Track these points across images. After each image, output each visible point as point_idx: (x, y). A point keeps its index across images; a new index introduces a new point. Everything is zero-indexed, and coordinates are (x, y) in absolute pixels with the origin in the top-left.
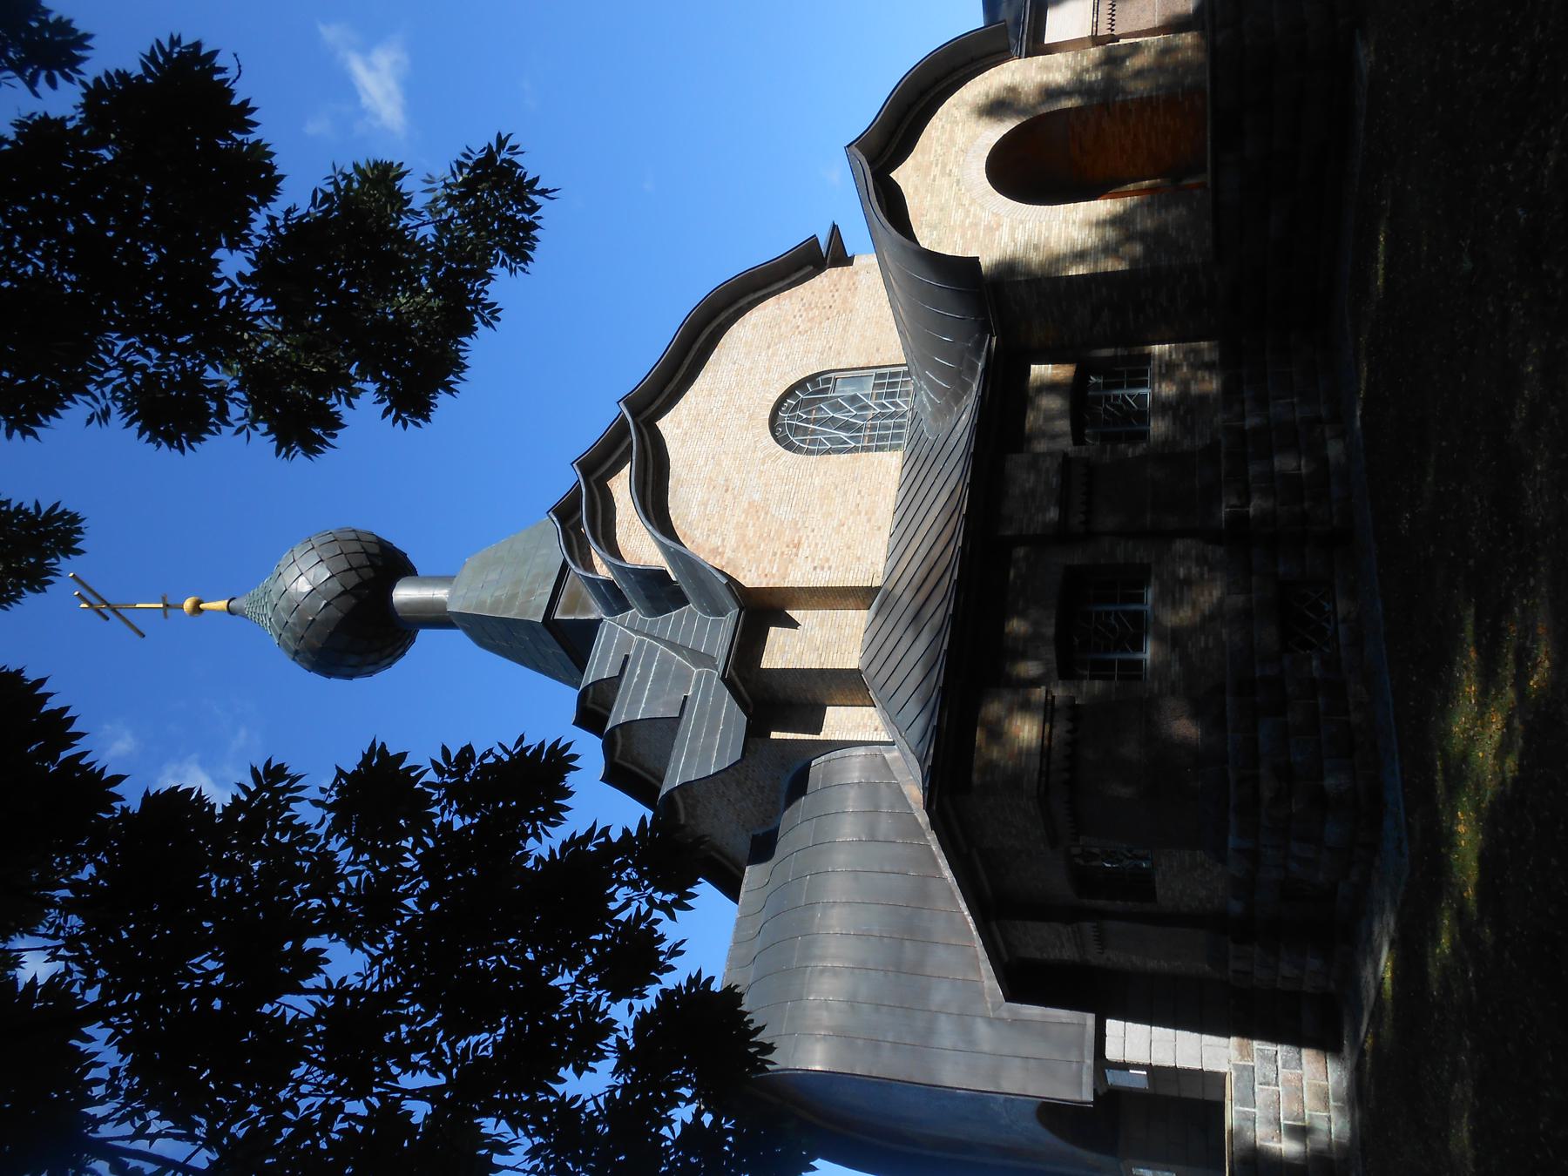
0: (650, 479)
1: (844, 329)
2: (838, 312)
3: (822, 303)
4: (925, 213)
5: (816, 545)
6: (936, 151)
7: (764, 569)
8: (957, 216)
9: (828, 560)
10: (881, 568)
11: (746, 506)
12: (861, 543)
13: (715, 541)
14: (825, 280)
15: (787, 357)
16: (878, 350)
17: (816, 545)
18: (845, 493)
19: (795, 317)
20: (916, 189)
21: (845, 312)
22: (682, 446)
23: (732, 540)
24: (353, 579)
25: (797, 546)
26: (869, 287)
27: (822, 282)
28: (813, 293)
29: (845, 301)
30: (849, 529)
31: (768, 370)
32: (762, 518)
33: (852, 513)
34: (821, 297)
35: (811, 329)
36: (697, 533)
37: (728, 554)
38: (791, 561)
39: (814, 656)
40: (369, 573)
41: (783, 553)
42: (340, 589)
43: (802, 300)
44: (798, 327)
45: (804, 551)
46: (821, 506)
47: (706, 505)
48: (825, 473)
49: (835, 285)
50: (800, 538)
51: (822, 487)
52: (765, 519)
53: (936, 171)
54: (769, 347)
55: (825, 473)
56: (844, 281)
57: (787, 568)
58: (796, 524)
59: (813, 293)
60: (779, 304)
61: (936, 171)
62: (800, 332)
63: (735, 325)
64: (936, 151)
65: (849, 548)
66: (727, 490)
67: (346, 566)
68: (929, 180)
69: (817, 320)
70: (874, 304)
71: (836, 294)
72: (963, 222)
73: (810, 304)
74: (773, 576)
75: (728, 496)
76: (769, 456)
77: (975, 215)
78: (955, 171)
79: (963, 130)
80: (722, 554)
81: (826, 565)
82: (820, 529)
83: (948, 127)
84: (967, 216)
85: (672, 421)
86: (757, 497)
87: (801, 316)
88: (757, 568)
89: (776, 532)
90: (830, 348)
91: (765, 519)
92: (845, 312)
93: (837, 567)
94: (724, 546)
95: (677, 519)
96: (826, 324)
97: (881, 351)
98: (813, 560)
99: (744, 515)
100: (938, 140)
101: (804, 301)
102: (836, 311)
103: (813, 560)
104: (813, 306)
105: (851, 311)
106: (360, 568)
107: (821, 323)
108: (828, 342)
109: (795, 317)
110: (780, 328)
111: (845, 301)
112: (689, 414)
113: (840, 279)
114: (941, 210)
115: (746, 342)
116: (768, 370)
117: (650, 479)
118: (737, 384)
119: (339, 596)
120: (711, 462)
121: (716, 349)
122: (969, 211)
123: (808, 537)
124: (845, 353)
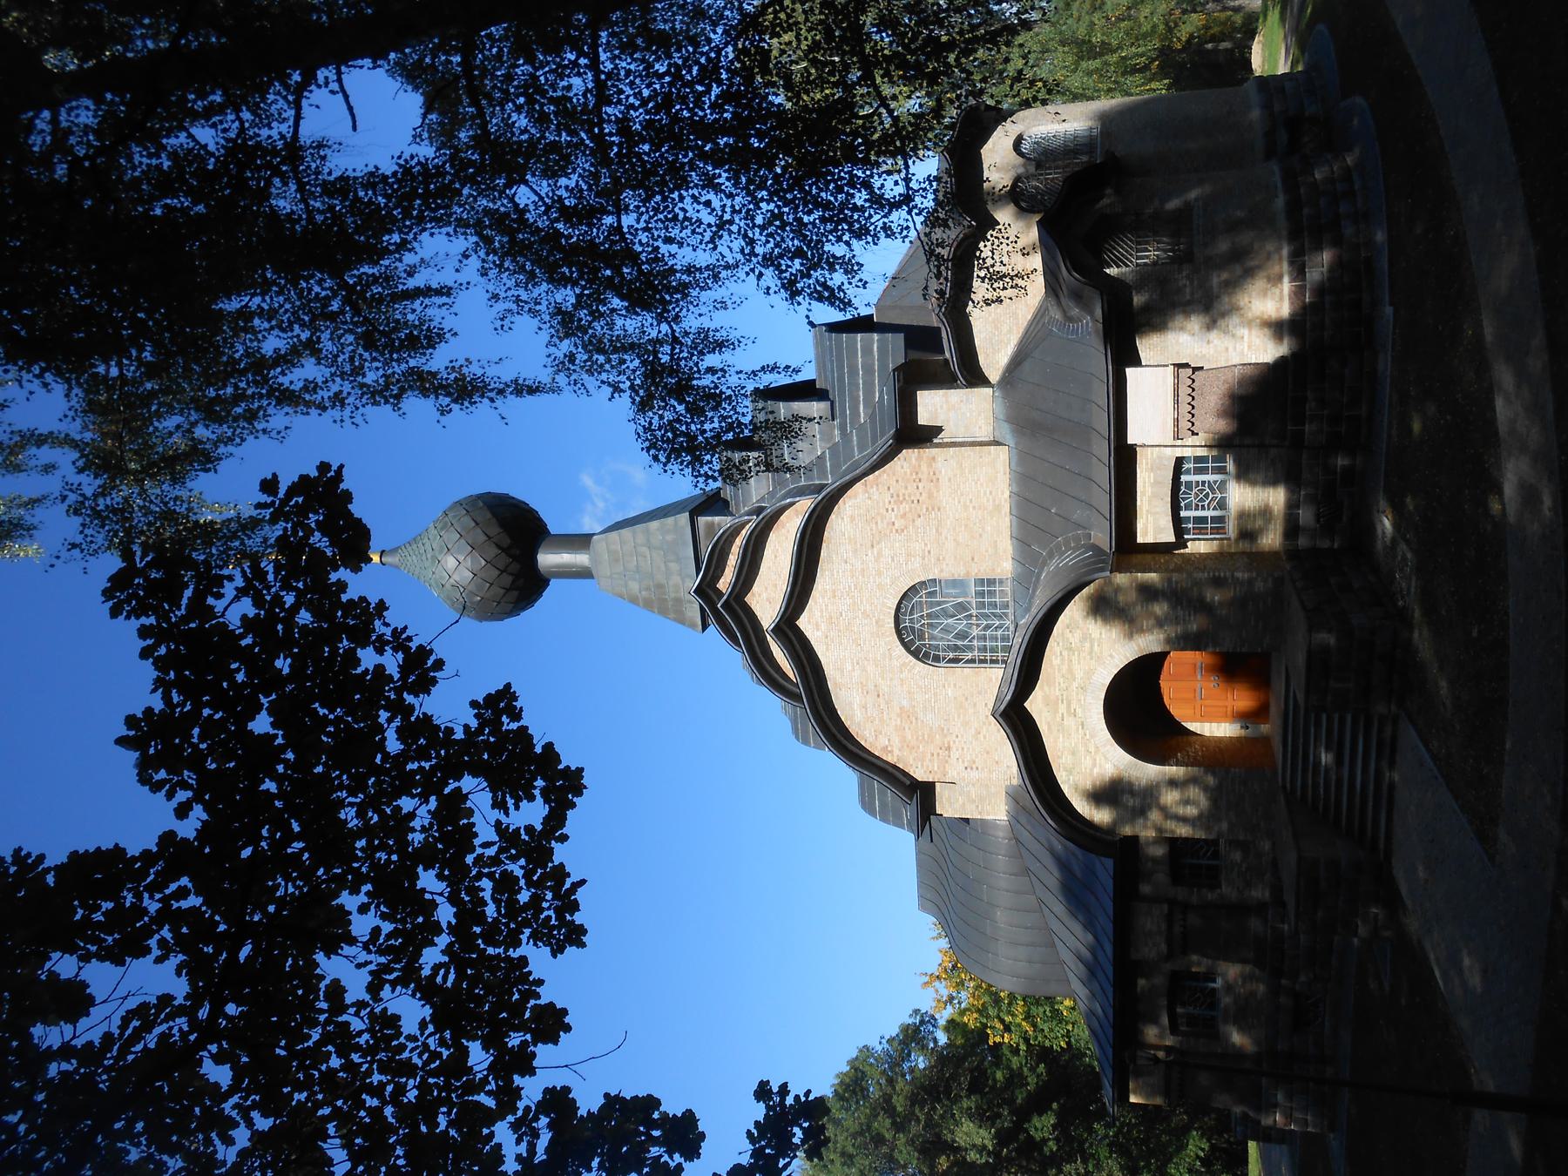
0: (812, 683)
1: (937, 530)
2: (927, 509)
3: (910, 496)
4: (1059, 754)
5: (963, 749)
6: (1059, 684)
7: (928, 767)
8: (1088, 762)
9: (974, 762)
10: (1015, 769)
11: (899, 711)
12: (996, 750)
13: (883, 741)
14: (906, 465)
15: (893, 560)
16: (973, 559)
17: (963, 749)
18: (975, 705)
19: (887, 510)
20: (1049, 728)
21: (933, 509)
22: (827, 649)
23: (896, 741)
24: (507, 580)
25: (949, 749)
26: (950, 480)
27: (902, 467)
28: (897, 481)
29: (930, 496)
30: (985, 737)
31: (879, 574)
32: (914, 721)
33: (984, 723)
34: (906, 488)
35: (906, 527)
36: (867, 733)
37: (896, 752)
38: (947, 762)
39: (974, 807)
40: (515, 567)
41: (938, 754)
42: (502, 591)
43: (889, 488)
44: (893, 524)
45: (955, 754)
46: (959, 717)
47: (865, 707)
48: (955, 685)
49: (917, 473)
50: (949, 743)
51: (955, 698)
52: (917, 723)
53: (1062, 708)
54: (872, 546)
55: (955, 685)
56: (924, 468)
57: (944, 767)
58: (943, 730)
59: (897, 481)
60: (867, 492)
61: (1062, 708)
62: (897, 531)
63: (833, 516)
64: (1059, 684)
65: (988, 753)
66: (878, 696)
67: (497, 572)
68: (1058, 719)
69: (909, 515)
70: (959, 502)
71: (920, 485)
72: (1092, 770)
73: (898, 496)
74: (936, 772)
75: (881, 700)
76: (904, 664)
77: (1100, 766)
78: (1079, 711)
79: (1079, 663)
80: (891, 752)
81: (974, 766)
82: (962, 736)
83: (1065, 653)
84: (1094, 765)
85: (809, 622)
86: (905, 703)
87: (893, 510)
88: (922, 765)
89: (929, 736)
90: (929, 552)
91: (917, 723)
92: (933, 509)
93: (982, 769)
94: (892, 746)
95: (846, 719)
96: (919, 522)
97: (976, 560)
98: (963, 762)
99: (899, 720)
100: (1059, 670)
101: (892, 491)
102: (924, 506)
103: (963, 762)
104: (901, 498)
105: (939, 509)
106: (507, 567)
107: (914, 521)
108: (926, 545)
109: (887, 510)
110: (877, 523)
111: (930, 496)
112: (822, 617)
113: (920, 466)
114: (1073, 753)
115: (850, 538)
116: (879, 574)
117: (812, 683)
118: (856, 588)
119: (504, 595)
120: (857, 667)
121: (824, 545)
122: (1095, 760)
123: (954, 742)
124: (944, 559)
